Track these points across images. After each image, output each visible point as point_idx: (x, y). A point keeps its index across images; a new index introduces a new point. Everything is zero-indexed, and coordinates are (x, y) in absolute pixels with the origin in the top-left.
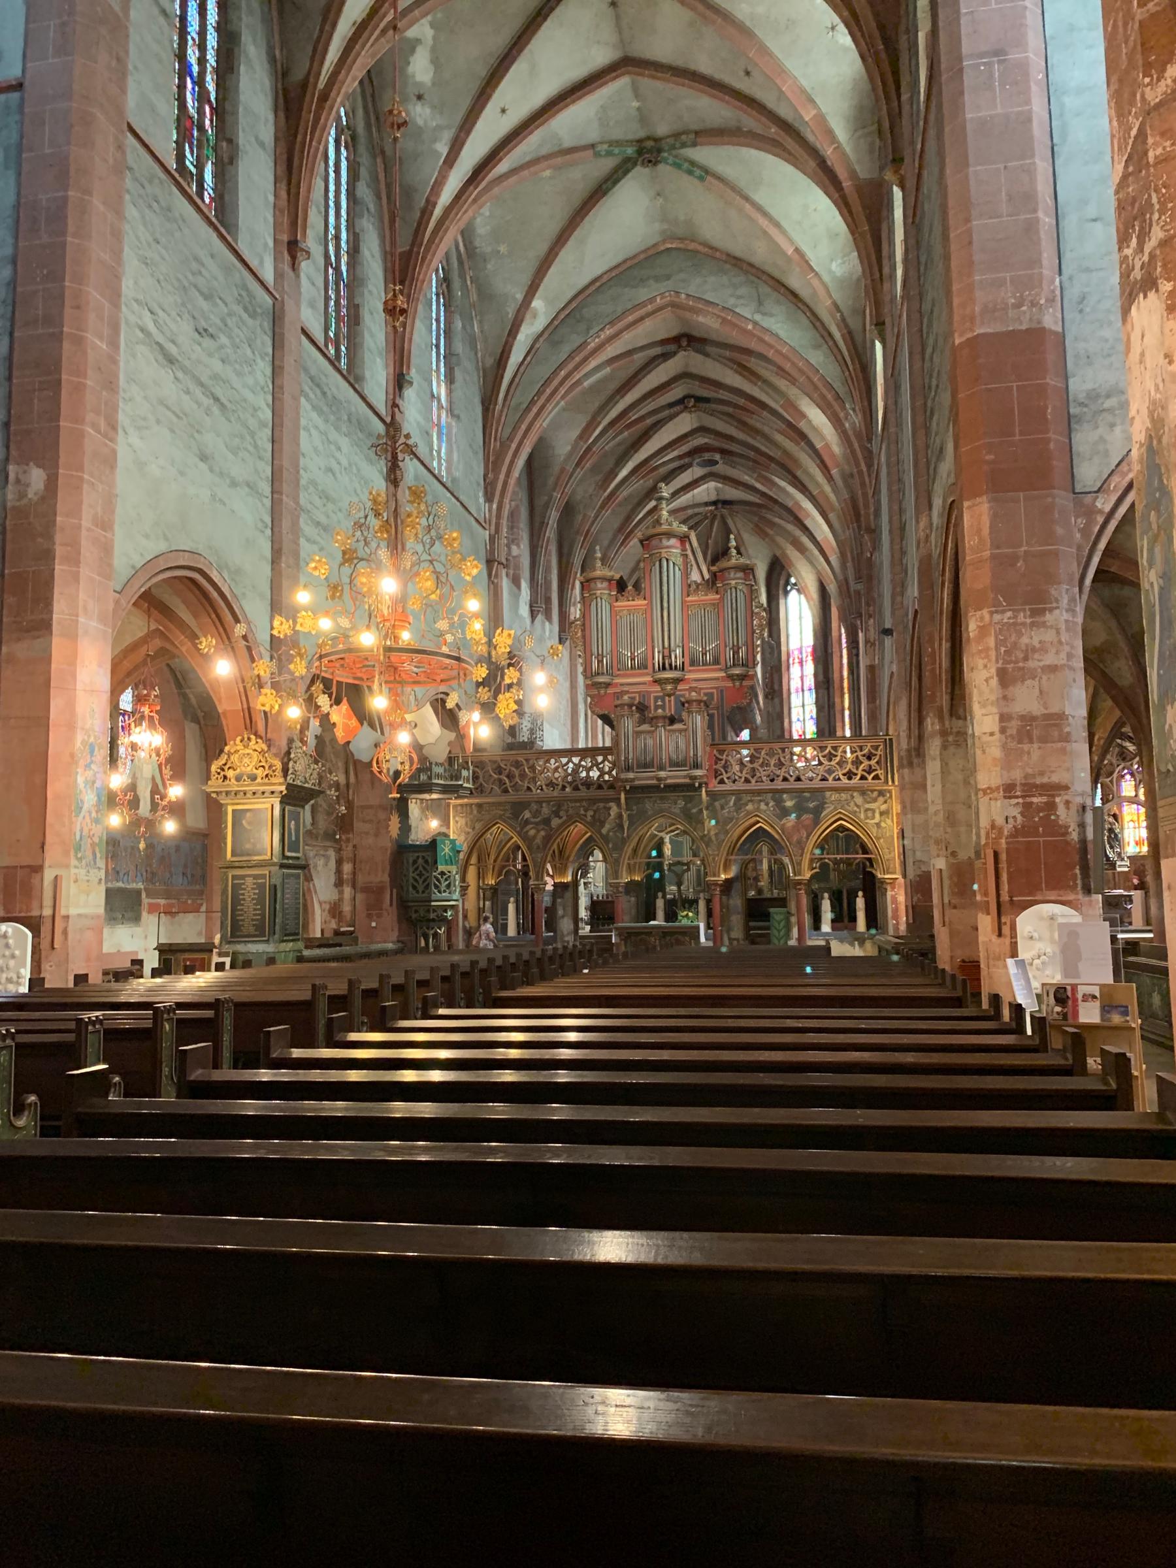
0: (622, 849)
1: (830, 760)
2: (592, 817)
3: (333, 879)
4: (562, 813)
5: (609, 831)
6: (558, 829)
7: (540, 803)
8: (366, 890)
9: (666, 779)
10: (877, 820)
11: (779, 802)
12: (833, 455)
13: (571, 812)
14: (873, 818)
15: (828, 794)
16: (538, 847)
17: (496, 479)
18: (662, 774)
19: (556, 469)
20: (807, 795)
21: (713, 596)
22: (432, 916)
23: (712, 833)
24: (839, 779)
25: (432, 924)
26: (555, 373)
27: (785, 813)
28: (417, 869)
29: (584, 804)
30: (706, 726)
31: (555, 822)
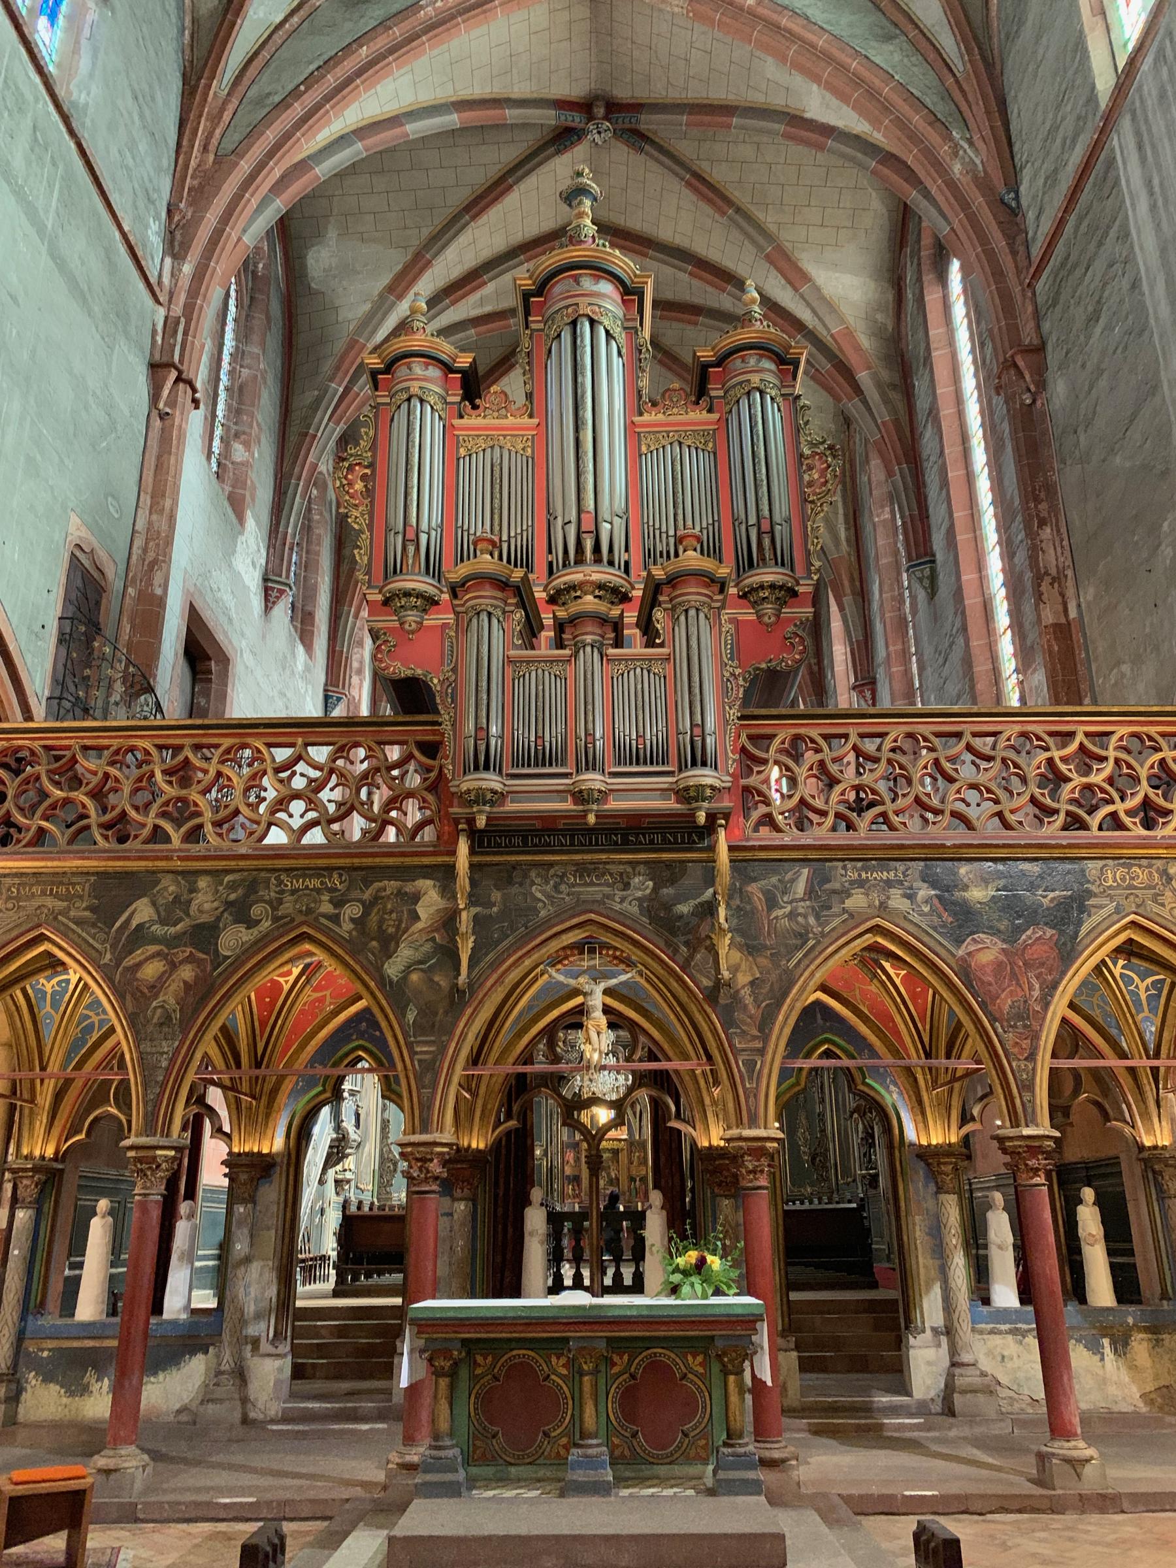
0: (451, 1033)
1: (1086, 770)
2: (359, 922)
4: (256, 911)
5: (408, 970)
6: (238, 962)
7: (190, 876)
9: (604, 795)
11: (946, 890)
12: (858, 348)
13: (288, 906)
15: (1092, 867)
16: (167, 1019)
17: (196, 221)
18: (593, 780)
19: (340, 346)
20: (1033, 868)
21: (699, 415)
23: (743, 979)
24: (1121, 826)
26: (348, 50)
30: (726, 653)
31: (232, 939)
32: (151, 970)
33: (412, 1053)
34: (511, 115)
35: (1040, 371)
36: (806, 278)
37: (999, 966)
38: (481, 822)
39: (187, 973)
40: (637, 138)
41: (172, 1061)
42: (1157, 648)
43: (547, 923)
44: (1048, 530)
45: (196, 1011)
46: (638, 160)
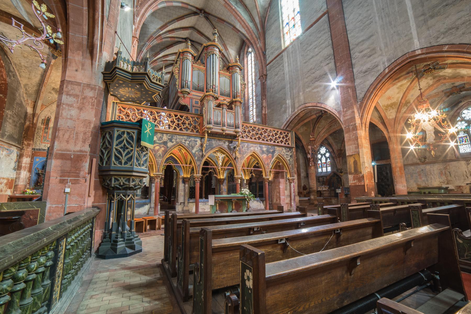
1: (276, 135)
3: (13, 165)
4: (173, 140)
5: (196, 152)
6: (171, 148)
8: (63, 157)
10: (289, 159)
11: (261, 148)
14: (288, 158)
15: (276, 147)
16: (160, 156)
20: (270, 147)
22: (132, 184)
25: (129, 192)
27: (263, 152)
28: (120, 143)
29: (185, 137)
31: (170, 144)
32: (157, 148)
33: (197, 164)
34: (189, 7)
35: (266, 78)
36: (228, 49)
37: (266, 158)
38: (209, 132)
39: (163, 149)
40: (207, 18)
41: (161, 162)
42: (279, 121)
43: (214, 148)
44: (264, 101)
45: (164, 155)
46: (205, 21)
